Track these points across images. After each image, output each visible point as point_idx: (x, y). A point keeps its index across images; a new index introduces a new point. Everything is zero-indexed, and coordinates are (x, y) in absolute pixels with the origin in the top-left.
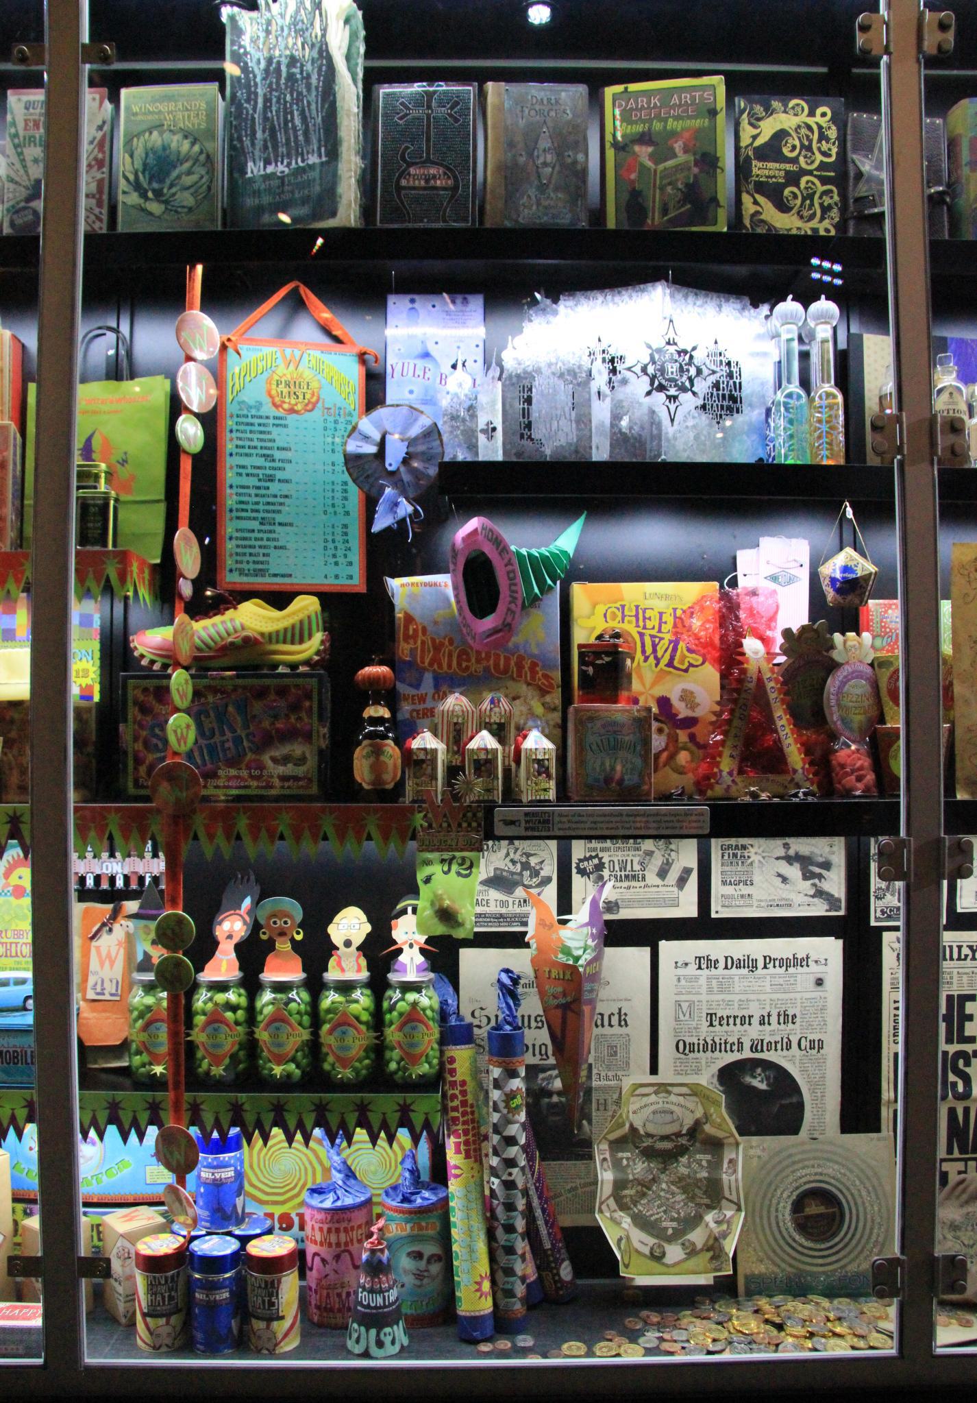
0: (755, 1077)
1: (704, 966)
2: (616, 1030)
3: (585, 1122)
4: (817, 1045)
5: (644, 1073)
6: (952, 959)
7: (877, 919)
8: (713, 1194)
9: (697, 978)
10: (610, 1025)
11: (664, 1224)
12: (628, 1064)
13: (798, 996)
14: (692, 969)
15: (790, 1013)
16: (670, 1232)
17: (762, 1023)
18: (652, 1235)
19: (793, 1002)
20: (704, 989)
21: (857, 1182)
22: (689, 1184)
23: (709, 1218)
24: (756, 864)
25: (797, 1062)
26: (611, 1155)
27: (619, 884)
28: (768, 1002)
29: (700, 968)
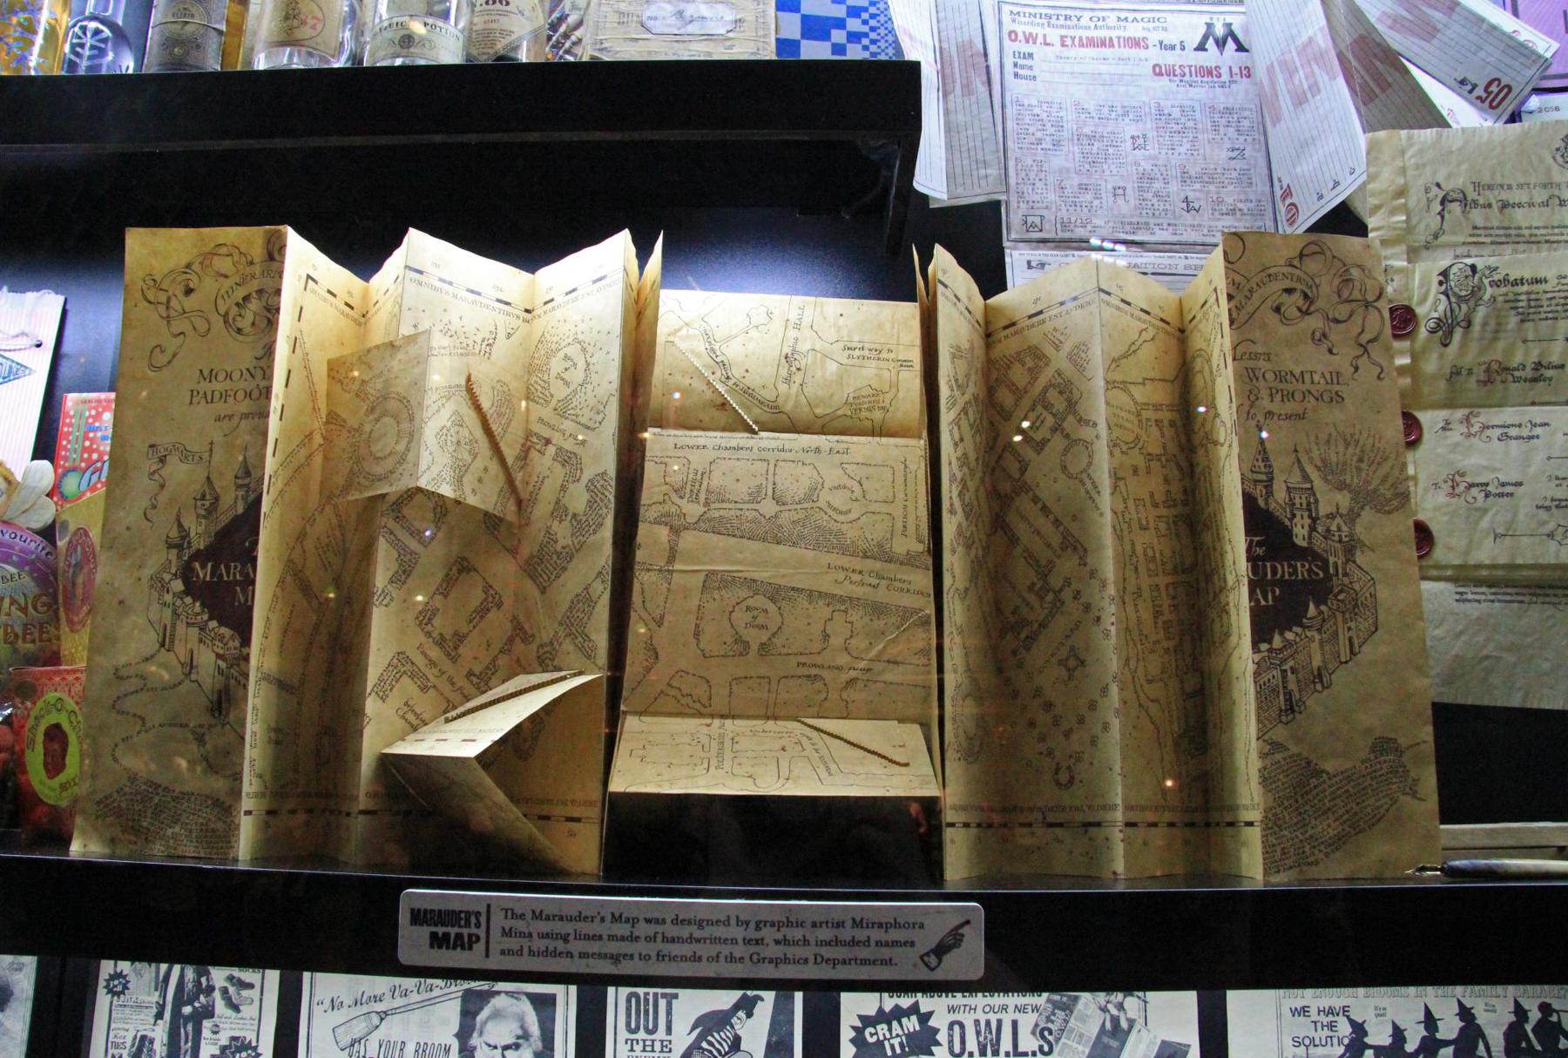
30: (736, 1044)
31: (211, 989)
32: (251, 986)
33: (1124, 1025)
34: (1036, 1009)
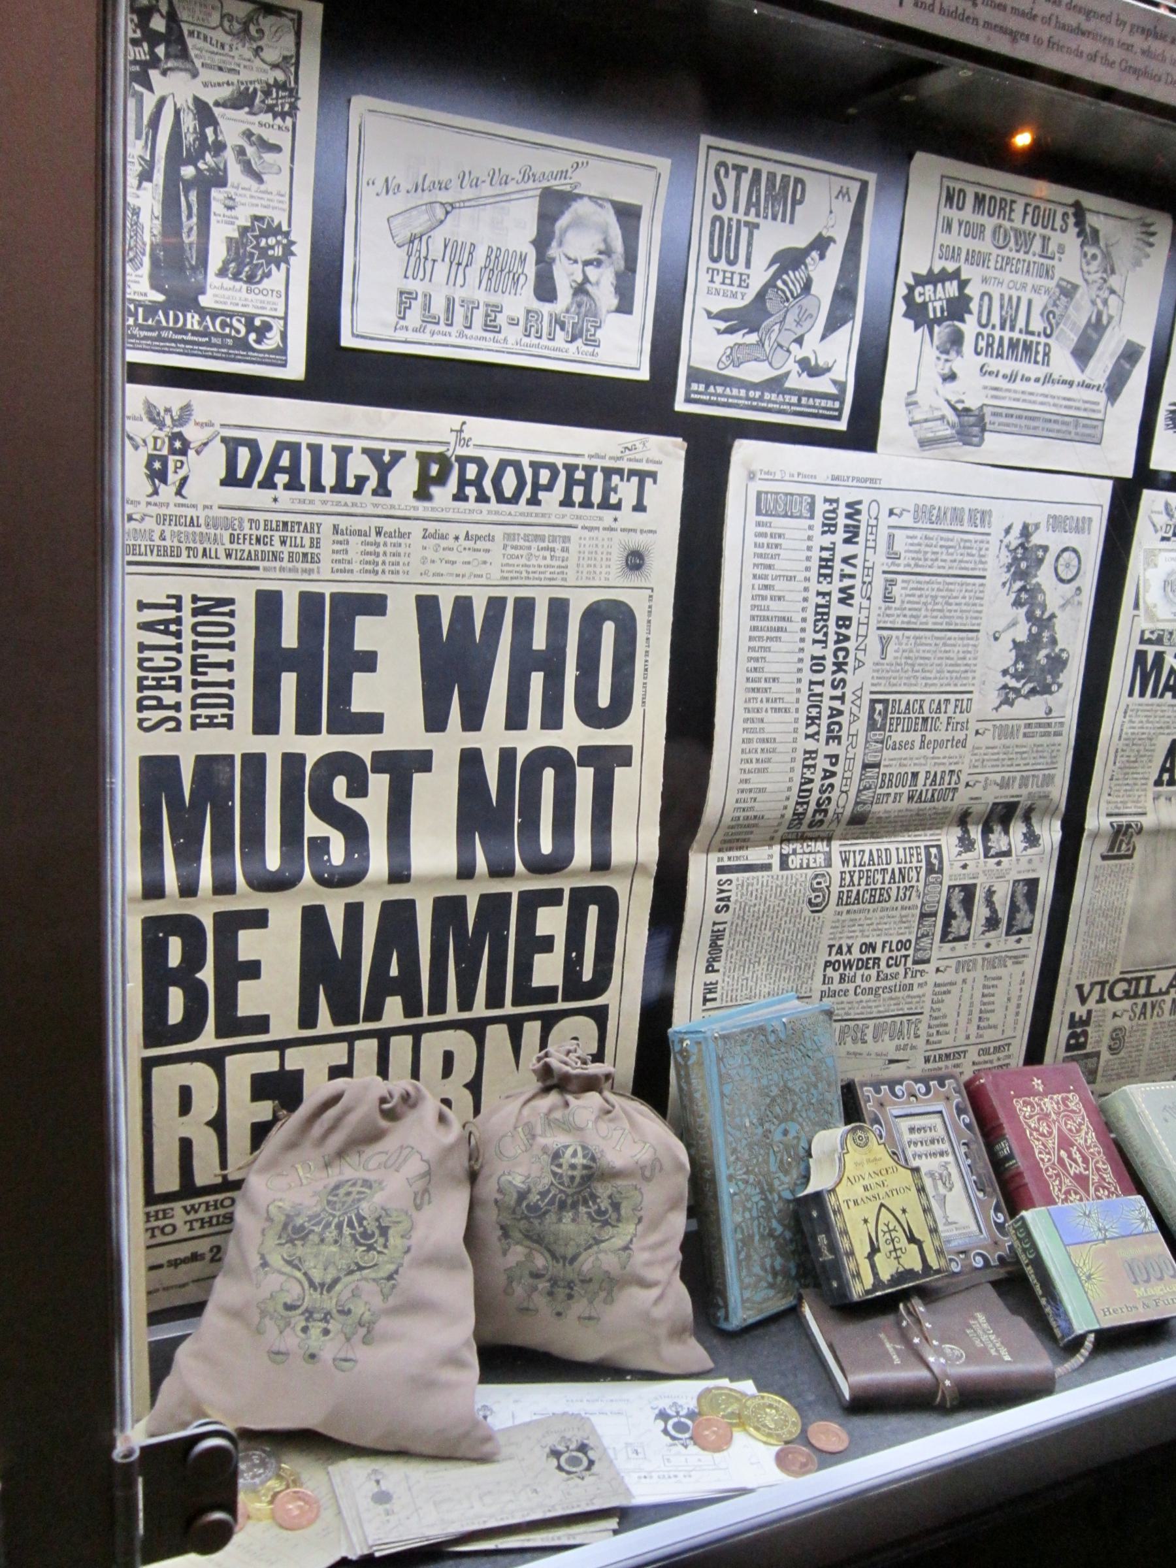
6: (317, 486)
30: (807, 287)
31: (219, 147)
32: (277, 149)
33: (1105, 320)
34: (1047, 291)
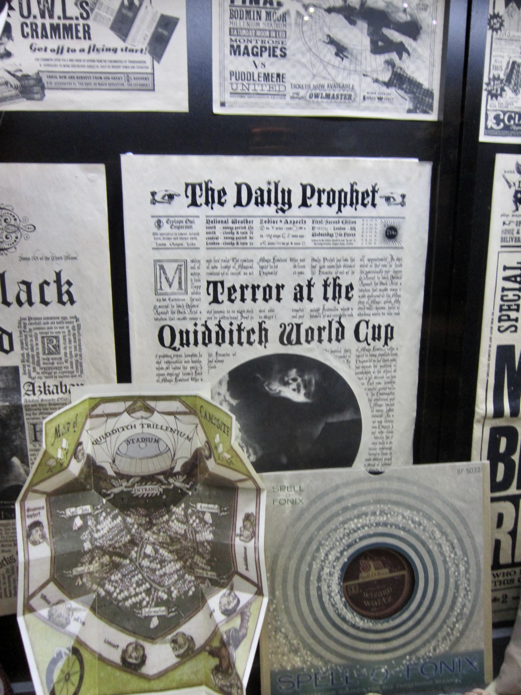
0: (286, 384)
1: (201, 200)
2: (54, 310)
3: (15, 460)
4: (385, 334)
5: (108, 381)
7: (489, 131)
8: (221, 566)
9: (189, 222)
10: (43, 301)
11: (145, 612)
12: (79, 365)
13: (356, 254)
14: (181, 206)
15: (344, 282)
16: (155, 622)
17: (298, 297)
18: (124, 629)
19: (349, 263)
20: (201, 241)
21: (438, 534)
22: (186, 549)
23: (216, 601)
24: (292, 18)
25: (353, 360)
26: (51, 515)
27: (40, 43)
28: (308, 263)
29: (194, 203)
